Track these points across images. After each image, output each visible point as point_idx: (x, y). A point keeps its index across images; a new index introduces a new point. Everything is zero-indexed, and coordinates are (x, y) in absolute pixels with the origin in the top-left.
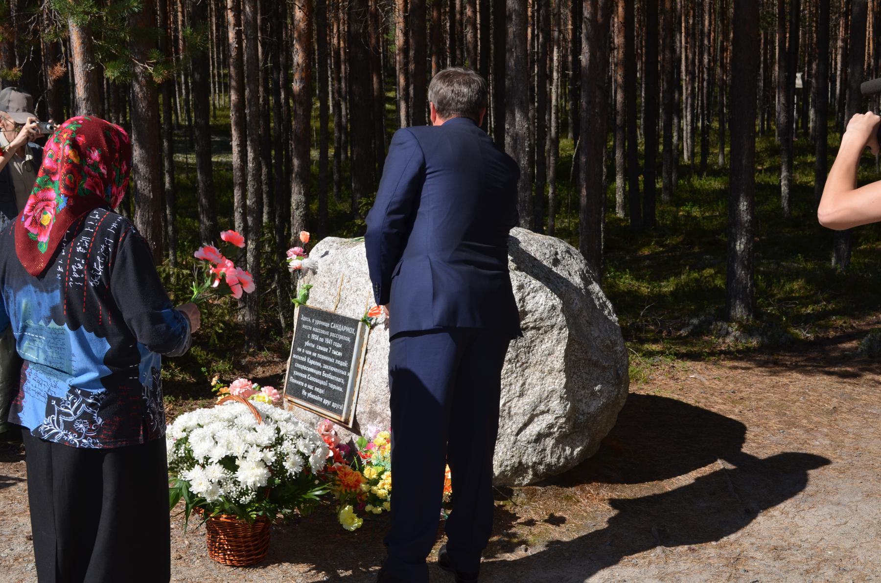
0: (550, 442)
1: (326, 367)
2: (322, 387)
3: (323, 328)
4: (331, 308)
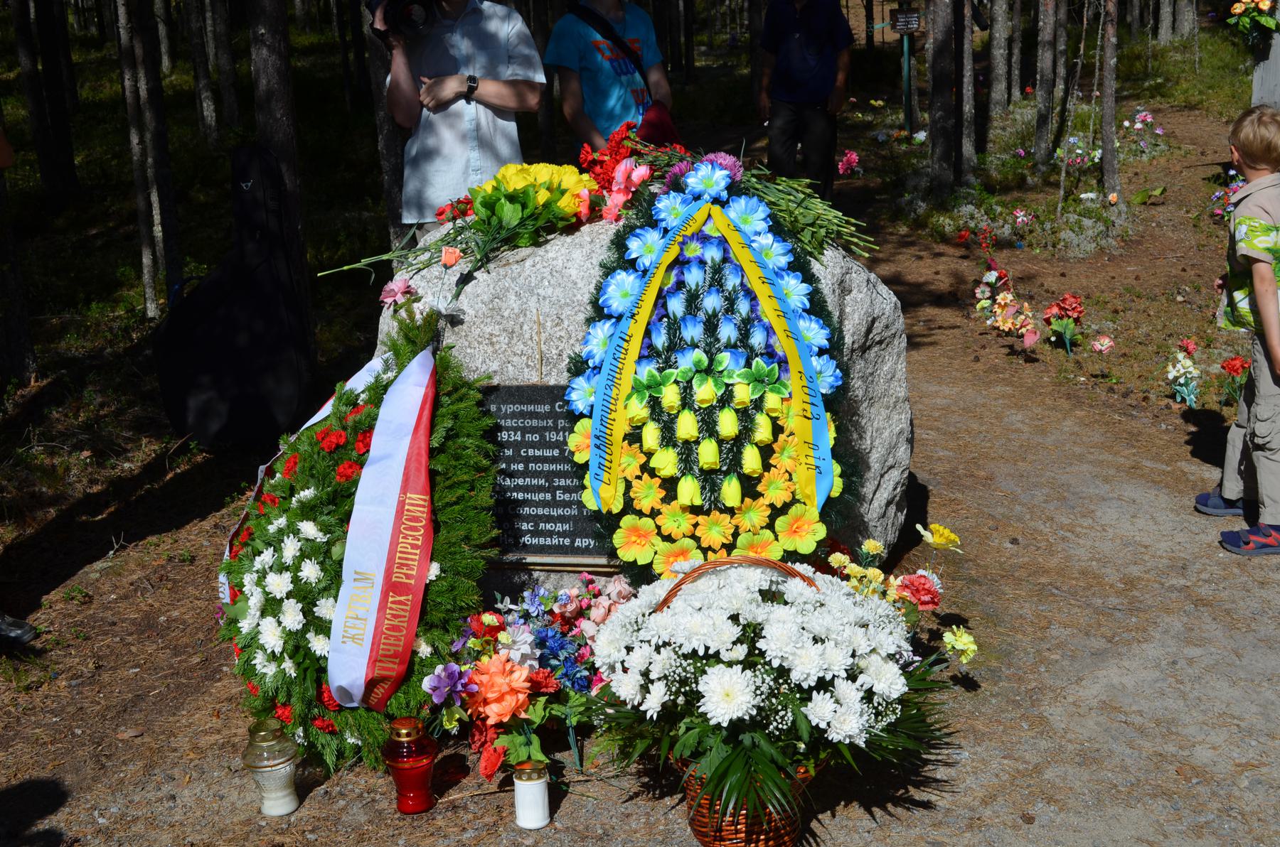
0: (893, 508)
1: (562, 482)
2: (562, 519)
3: (522, 415)
4: (533, 378)
